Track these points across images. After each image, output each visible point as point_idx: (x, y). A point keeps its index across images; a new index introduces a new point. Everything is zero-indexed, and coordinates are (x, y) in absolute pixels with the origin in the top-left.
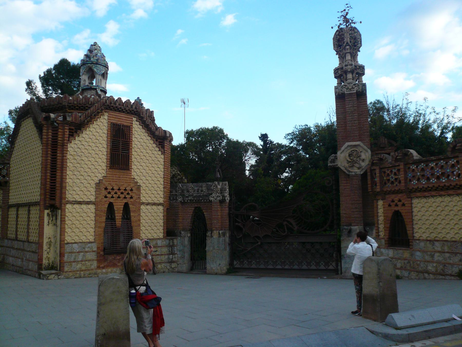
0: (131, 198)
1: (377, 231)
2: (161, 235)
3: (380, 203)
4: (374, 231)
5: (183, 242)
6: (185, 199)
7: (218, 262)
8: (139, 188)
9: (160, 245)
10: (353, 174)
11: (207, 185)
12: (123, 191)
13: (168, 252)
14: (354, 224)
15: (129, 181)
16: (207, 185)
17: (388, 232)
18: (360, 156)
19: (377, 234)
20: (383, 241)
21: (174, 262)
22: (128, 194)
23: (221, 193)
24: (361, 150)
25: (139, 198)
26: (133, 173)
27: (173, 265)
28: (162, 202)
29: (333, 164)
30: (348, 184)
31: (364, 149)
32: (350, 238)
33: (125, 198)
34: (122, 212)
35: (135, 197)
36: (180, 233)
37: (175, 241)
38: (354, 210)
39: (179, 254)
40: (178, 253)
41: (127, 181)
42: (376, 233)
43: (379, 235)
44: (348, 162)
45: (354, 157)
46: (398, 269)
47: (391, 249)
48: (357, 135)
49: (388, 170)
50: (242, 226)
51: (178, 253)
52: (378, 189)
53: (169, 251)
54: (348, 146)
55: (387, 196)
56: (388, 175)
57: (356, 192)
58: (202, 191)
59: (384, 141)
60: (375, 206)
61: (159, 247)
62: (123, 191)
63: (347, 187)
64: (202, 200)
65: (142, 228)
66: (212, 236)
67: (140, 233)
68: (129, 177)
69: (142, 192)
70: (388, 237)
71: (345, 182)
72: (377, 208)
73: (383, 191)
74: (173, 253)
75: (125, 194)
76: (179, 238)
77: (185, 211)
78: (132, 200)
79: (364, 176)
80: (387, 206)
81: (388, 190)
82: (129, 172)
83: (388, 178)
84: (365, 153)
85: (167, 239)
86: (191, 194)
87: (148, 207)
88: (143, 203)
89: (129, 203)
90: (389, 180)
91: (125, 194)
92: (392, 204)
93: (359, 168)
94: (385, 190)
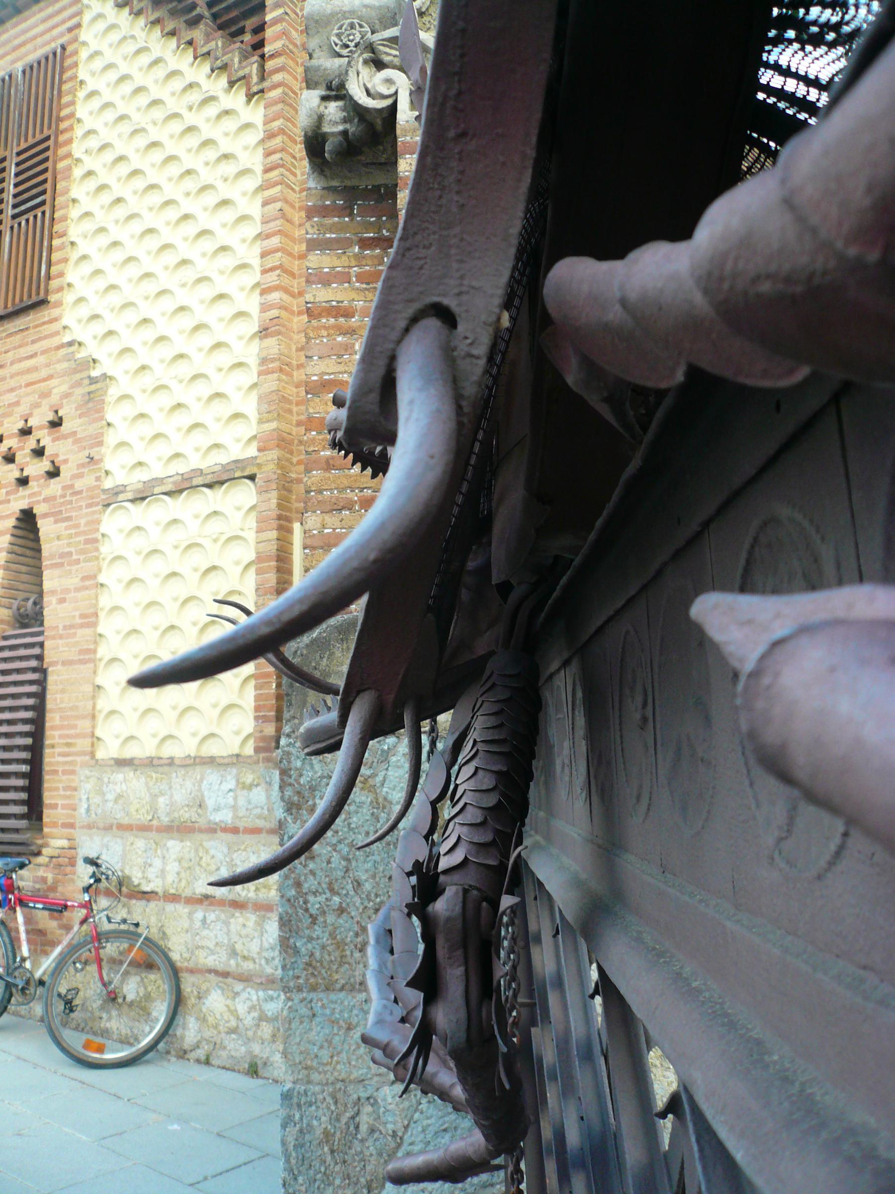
0: (54, 473)
9: (225, 817)
15: (44, 373)
22: (39, 452)
41: (34, 377)
61: (212, 830)
69: (110, 416)
78: (55, 486)
82: (44, 314)
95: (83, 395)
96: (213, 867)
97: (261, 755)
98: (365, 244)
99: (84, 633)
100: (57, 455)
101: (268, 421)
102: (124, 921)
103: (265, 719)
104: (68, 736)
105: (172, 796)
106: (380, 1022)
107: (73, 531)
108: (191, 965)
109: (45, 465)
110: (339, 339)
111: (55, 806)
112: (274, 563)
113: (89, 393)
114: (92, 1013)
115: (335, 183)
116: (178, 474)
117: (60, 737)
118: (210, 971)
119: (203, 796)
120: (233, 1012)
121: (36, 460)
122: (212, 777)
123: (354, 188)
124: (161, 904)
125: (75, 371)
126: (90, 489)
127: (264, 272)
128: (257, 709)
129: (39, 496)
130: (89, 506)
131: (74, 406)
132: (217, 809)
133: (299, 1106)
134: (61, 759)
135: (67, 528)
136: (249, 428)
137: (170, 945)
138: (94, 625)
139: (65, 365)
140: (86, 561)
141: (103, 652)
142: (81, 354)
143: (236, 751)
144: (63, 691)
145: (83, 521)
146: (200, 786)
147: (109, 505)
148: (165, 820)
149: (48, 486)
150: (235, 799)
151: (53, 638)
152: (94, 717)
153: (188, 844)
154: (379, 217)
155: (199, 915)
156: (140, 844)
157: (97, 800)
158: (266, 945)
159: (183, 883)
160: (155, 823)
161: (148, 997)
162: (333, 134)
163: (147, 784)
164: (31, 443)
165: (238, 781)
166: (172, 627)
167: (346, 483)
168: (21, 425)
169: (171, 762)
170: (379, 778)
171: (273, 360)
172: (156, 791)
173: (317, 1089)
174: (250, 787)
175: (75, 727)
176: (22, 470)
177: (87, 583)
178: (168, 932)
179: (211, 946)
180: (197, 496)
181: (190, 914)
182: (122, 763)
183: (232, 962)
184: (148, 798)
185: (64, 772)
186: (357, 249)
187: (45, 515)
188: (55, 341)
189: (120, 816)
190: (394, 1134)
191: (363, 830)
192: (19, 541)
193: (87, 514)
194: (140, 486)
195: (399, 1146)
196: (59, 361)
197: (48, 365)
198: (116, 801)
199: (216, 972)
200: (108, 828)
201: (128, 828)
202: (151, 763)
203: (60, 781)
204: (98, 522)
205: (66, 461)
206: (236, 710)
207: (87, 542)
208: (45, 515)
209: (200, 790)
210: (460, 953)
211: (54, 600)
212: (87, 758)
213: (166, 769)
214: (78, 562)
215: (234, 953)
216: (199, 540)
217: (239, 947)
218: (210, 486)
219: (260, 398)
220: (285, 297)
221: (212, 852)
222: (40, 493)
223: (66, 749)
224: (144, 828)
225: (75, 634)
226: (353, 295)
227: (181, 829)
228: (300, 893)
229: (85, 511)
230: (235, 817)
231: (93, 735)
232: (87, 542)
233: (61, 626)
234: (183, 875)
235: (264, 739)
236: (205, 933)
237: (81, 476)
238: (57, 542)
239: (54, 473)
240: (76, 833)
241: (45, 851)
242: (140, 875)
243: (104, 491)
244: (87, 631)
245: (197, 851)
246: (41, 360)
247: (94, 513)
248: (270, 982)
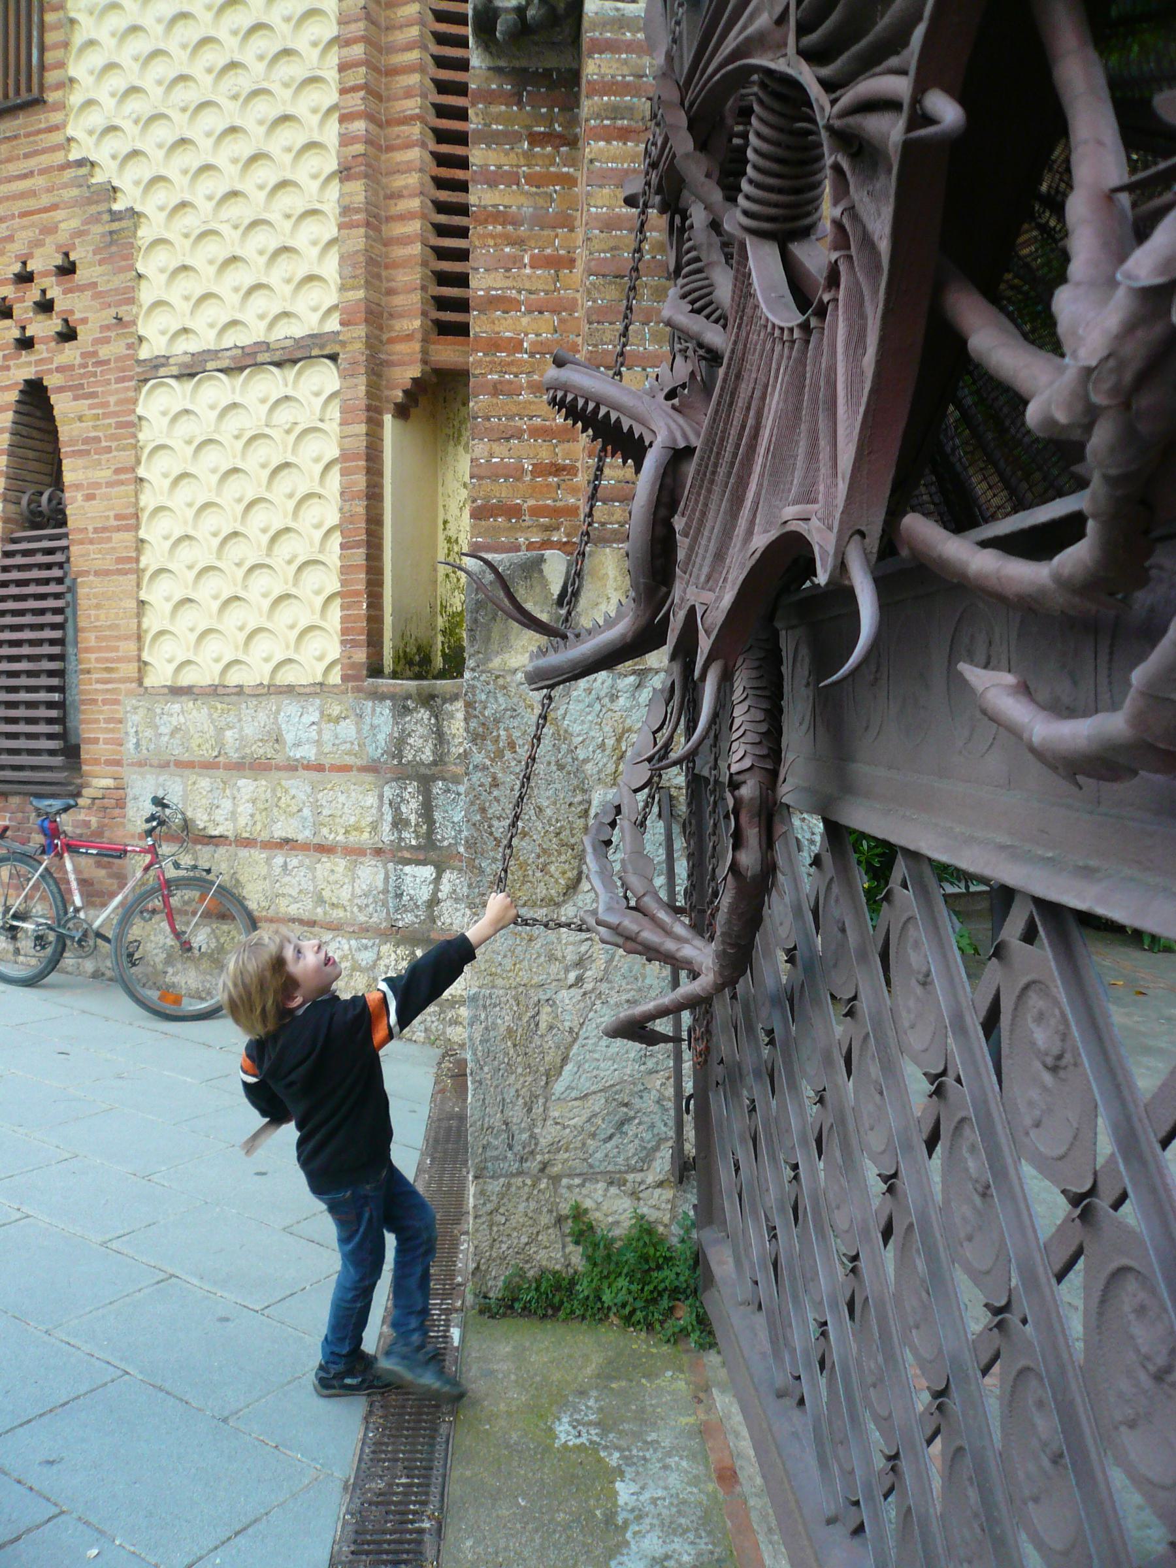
0: (68, 335)
8: (119, 231)
9: (308, 752)
13: (387, 834)
15: (45, 200)
22: (45, 306)
28: (333, 324)
53: (399, 823)
61: (293, 767)
68: (45, 160)
78: (70, 353)
85: (377, 696)
89: (50, 381)
95: (103, 235)
96: (295, 809)
97: (350, 685)
98: (534, 139)
100: (72, 312)
101: (353, 288)
102: (195, 867)
103: (354, 644)
104: (107, 660)
105: (242, 729)
106: (609, 909)
107: (100, 411)
108: (271, 913)
109: (54, 324)
110: (507, 250)
111: (96, 741)
112: (363, 463)
113: (111, 233)
114: (154, 966)
115: (502, 63)
116: (236, 347)
117: (97, 660)
118: (293, 920)
119: (279, 729)
121: (41, 317)
122: (291, 708)
123: (525, 70)
124: (232, 848)
125: (90, 201)
126: (118, 359)
127: (343, 91)
128: (344, 631)
129: (51, 363)
130: (120, 380)
131: (91, 248)
132: (297, 745)
133: (485, 1007)
134: (99, 686)
135: (91, 407)
136: (329, 296)
137: (245, 893)
138: (137, 527)
139: (75, 192)
140: (118, 449)
141: (149, 560)
142: (99, 178)
143: (319, 679)
144: (98, 607)
145: (112, 400)
146: (276, 718)
147: (146, 380)
148: (235, 756)
149: (62, 351)
150: (320, 733)
151: (81, 542)
152: (139, 638)
153: (264, 783)
154: (551, 108)
155: (279, 860)
156: (204, 783)
157: (149, 733)
158: (358, 892)
159: (258, 827)
160: (221, 759)
161: (221, 949)
162: (506, 10)
163: (210, 715)
164: (33, 294)
165: (322, 713)
166: (236, 534)
167: (515, 410)
168: (17, 268)
169: (240, 690)
170: (561, 712)
171: (357, 211)
172: (222, 724)
173: (501, 992)
174: (337, 720)
175: (116, 649)
176: (23, 328)
177: (123, 477)
178: (241, 879)
179: (294, 894)
180: (263, 376)
181: (268, 861)
182: (177, 691)
183: (319, 910)
184: (212, 732)
185: (105, 702)
186: (526, 145)
188: (58, 158)
189: (178, 752)
190: (571, 1030)
191: (545, 760)
192: (26, 419)
193: (117, 391)
194: (188, 359)
195: (575, 1040)
196: (65, 186)
197: (49, 190)
198: (172, 734)
199: (301, 922)
200: (164, 765)
201: (190, 765)
202: (216, 692)
203: (101, 712)
204: (135, 401)
205: (84, 321)
206: (317, 632)
207: (120, 425)
208: (60, 389)
209: (276, 722)
210: (756, 820)
211: (79, 497)
212: (134, 685)
213: (234, 698)
214: (109, 450)
215: (320, 901)
216: (267, 431)
217: (326, 894)
218: (278, 364)
219: (342, 258)
220: (372, 127)
221: (293, 792)
222: (51, 360)
223: (106, 675)
224: (209, 766)
225: (109, 539)
226: (522, 200)
227: (256, 767)
228: (485, 819)
229: (114, 386)
230: (320, 753)
231: (139, 659)
232: (120, 425)
233: (90, 528)
234: (258, 817)
235: (353, 666)
236: (287, 879)
237: (107, 341)
238: (78, 424)
240: (124, 771)
241: (85, 792)
242: (205, 817)
243: (139, 362)
244: (128, 536)
245: (274, 791)
246: (38, 182)
247: (127, 389)
248: (364, 930)
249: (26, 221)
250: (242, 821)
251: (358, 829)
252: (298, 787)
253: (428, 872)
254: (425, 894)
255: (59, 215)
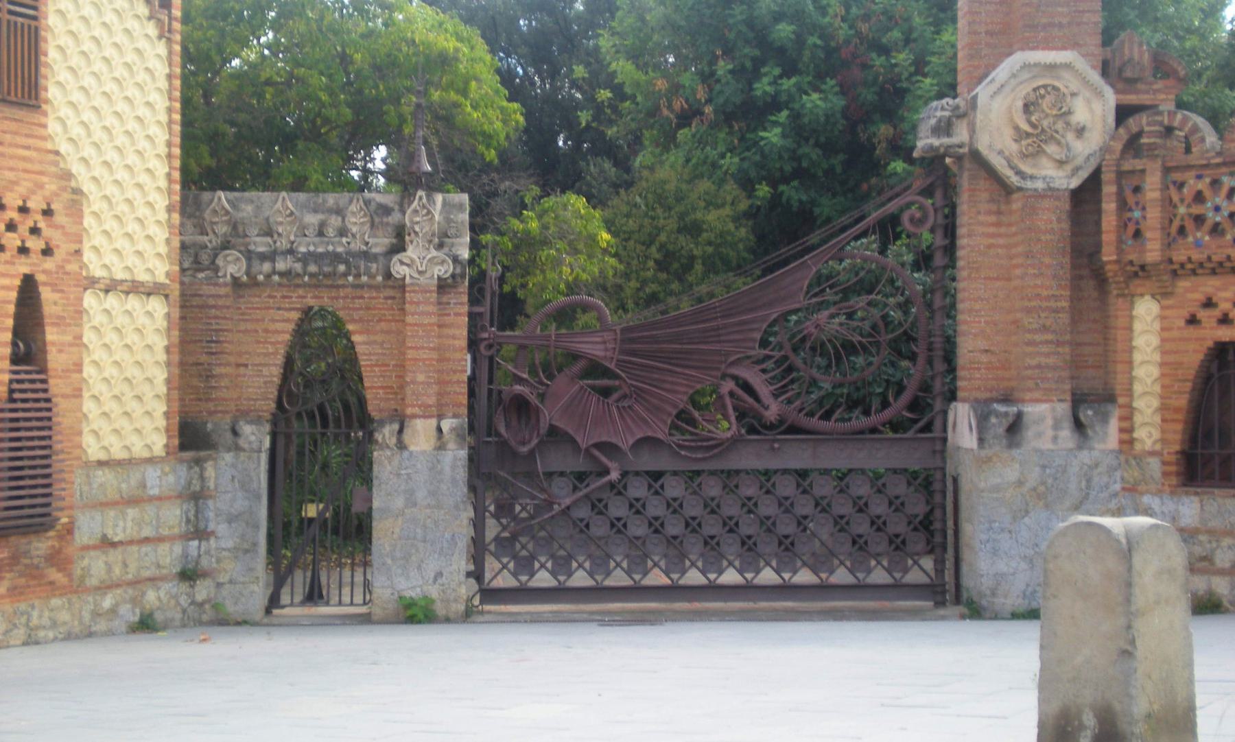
0: (47, 252)
1: (1125, 424)
2: (159, 443)
3: (1146, 311)
4: (1114, 425)
5: (240, 476)
6: (254, 270)
7: (431, 567)
9: (155, 491)
10: (1040, 185)
11: (367, 203)
12: (15, 215)
14: (1037, 395)
15: (37, 167)
16: (367, 203)
17: (1179, 427)
18: (1069, 113)
19: (1125, 436)
20: (1154, 465)
21: (204, 575)
22: (35, 231)
23: (440, 246)
24: (1074, 85)
25: (78, 252)
26: (53, 127)
27: (203, 590)
29: (946, 141)
30: (1003, 230)
31: (1085, 82)
32: (1015, 452)
33: (23, 250)
34: (10, 322)
35: (63, 249)
36: (235, 433)
37: (210, 471)
38: (1038, 338)
39: (225, 536)
40: (222, 529)
41: (29, 166)
42: (1122, 430)
43: (1131, 442)
44: (1020, 135)
45: (1041, 118)
46: (1221, 572)
47: (1187, 493)
48: (1065, 21)
49: (1199, 177)
50: (533, 399)
51: (222, 529)
52: (1153, 252)
53: (188, 521)
54: (1026, 66)
55: (1183, 284)
56: (1199, 197)
57: (1047, 260)
58: (343, 232)
59: (1136, 56)
60: (1121, 322)
61: (152, 499)
62: (15, 215)
63: (1001, 241)
64: (345, 275)
65: (89, 406)
66: (401, 446)
67: (80, 433)
68: (40, 144)
70: (1177, 448)
71: (993, 219)
72: (1130, 329)
73: (1171, 261)
74: (199, 533)
75: (24, 229)
76: (228, 457)
77: (250, 326)
78: (49, 264)
79: (1085, 197)
80: (1182, 323)
81: (1196, 256)
83: (1196, 210)
84: (1088, 101)
85: (181, 461)
86: (283, 244)
87: (112, 301)
88: (92, 282)
89: (40, 278)
90: (1199, 220)
91: (24, 229)
92: (1202, 314)
93: (1061, 163)
94: (1179, 256)
99: (75, 376)
109: (41, 245)
120: (159, 599)
130: (75, 286)
138: (80, 371)
139: (53, 169)
156: (112, 513)
168: (20, 203)
174: (166, 474)
182: (101, 464)
187: (45, 284)
188: (40, 144)
189: (102, 498)
197: (41, 162)
204: (81, 299)
208: (45, 284)
214: (69, 325)
215: (159, 566)
227: (133, 501)
237: (69, 262)
239: (47, 252)
249: (26, 176)
250: (128, 531)
251: (173, 527)
252: (150, 510)
253: (196, 543)
254: (195, 553)
255: (45, 179)
